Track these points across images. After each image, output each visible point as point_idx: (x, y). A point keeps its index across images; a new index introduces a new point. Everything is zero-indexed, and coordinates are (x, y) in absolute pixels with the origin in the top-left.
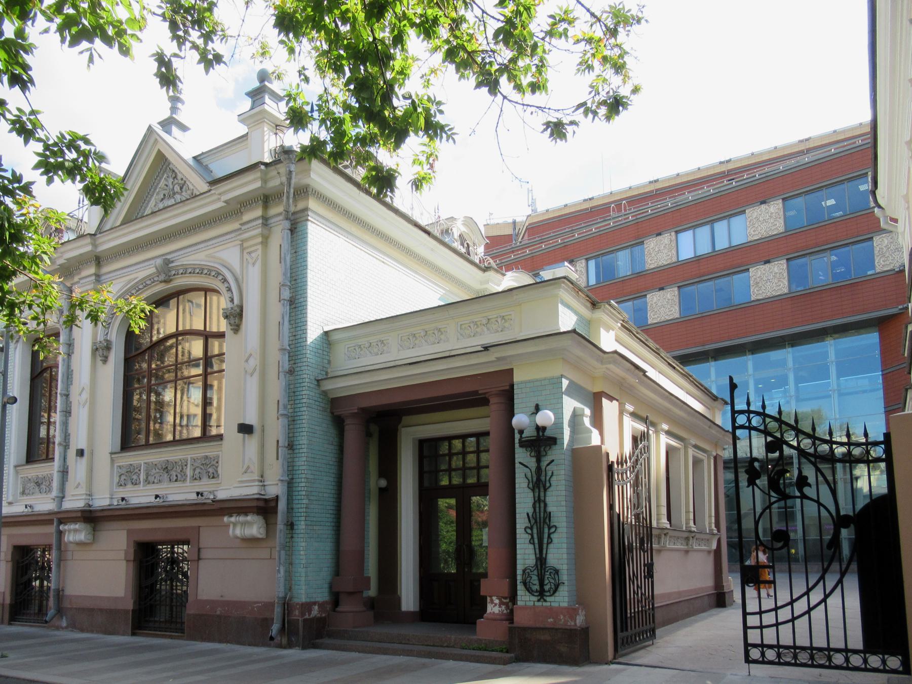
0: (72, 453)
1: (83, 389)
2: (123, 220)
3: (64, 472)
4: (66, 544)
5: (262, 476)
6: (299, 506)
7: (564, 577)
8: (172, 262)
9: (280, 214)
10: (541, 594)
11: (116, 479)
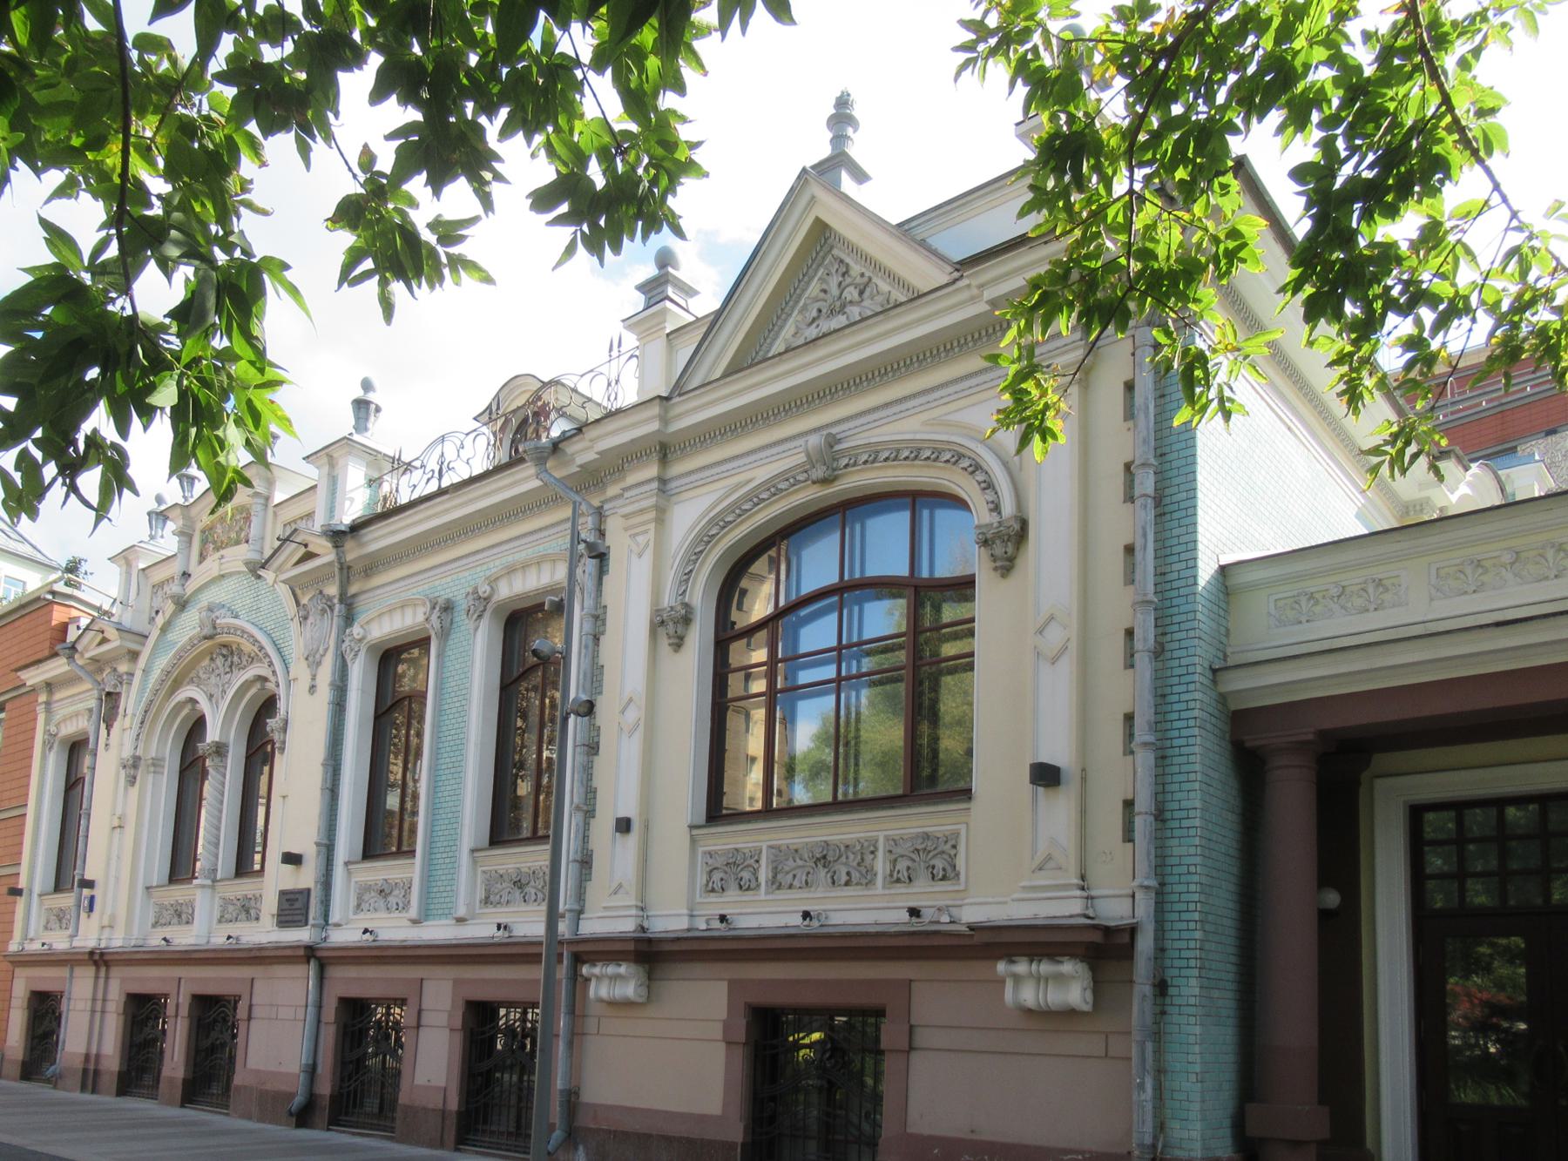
2: (725, 370)
11: (701, 879)
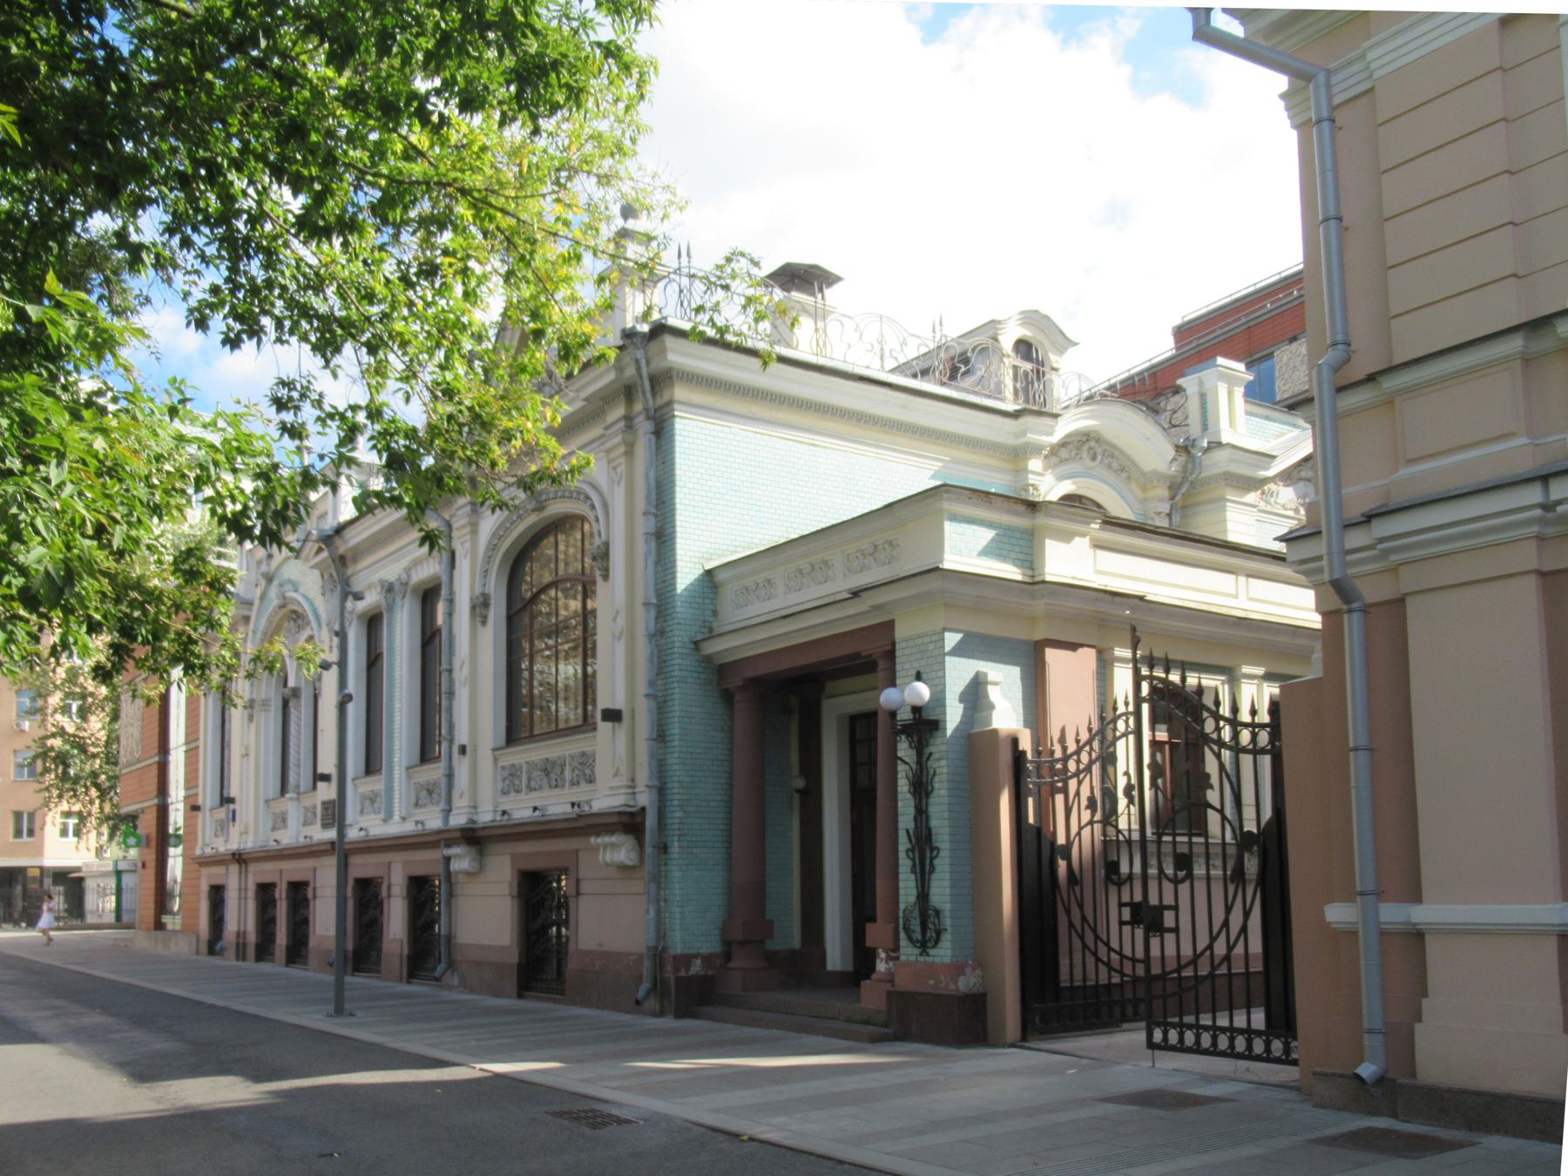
0: (455, 749)
3: (450, 776)
5: (633, 780)
7: (947, 922)
10: (923, 945)
11: (500, 785)
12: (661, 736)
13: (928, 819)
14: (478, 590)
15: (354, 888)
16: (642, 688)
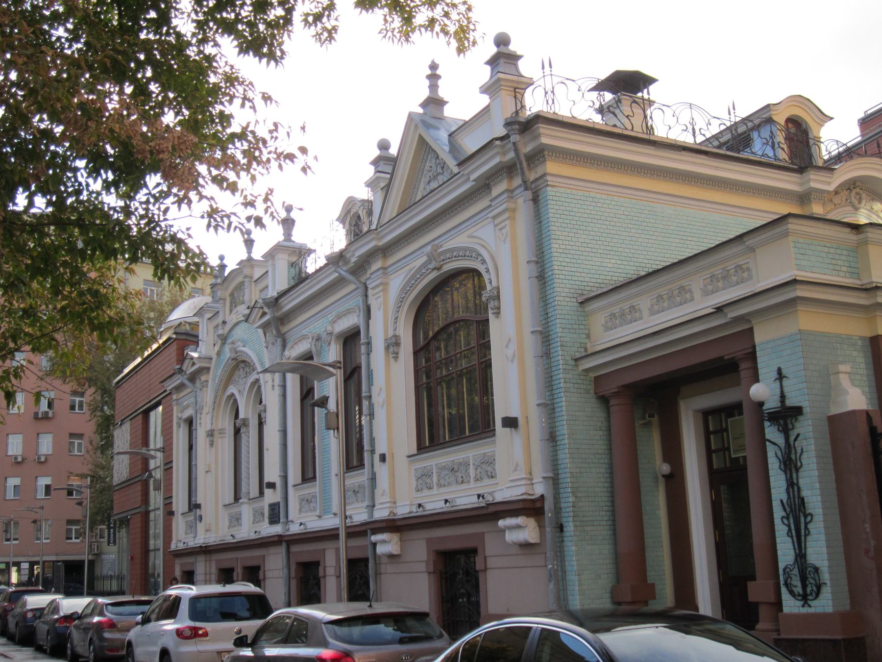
0: (377, 457)
1: (510, 340)
3: (373, 479)
4: (380, 557)
5: (531, 474)
6: (566, 505)
7: (826, 576)
8: (441, 246)
9: (519, 186)
10: (805, 598)
12: (552, 438)
13: (799, 489)
14: (390, 334)
15: (296, 570)
16: (533, 399)
